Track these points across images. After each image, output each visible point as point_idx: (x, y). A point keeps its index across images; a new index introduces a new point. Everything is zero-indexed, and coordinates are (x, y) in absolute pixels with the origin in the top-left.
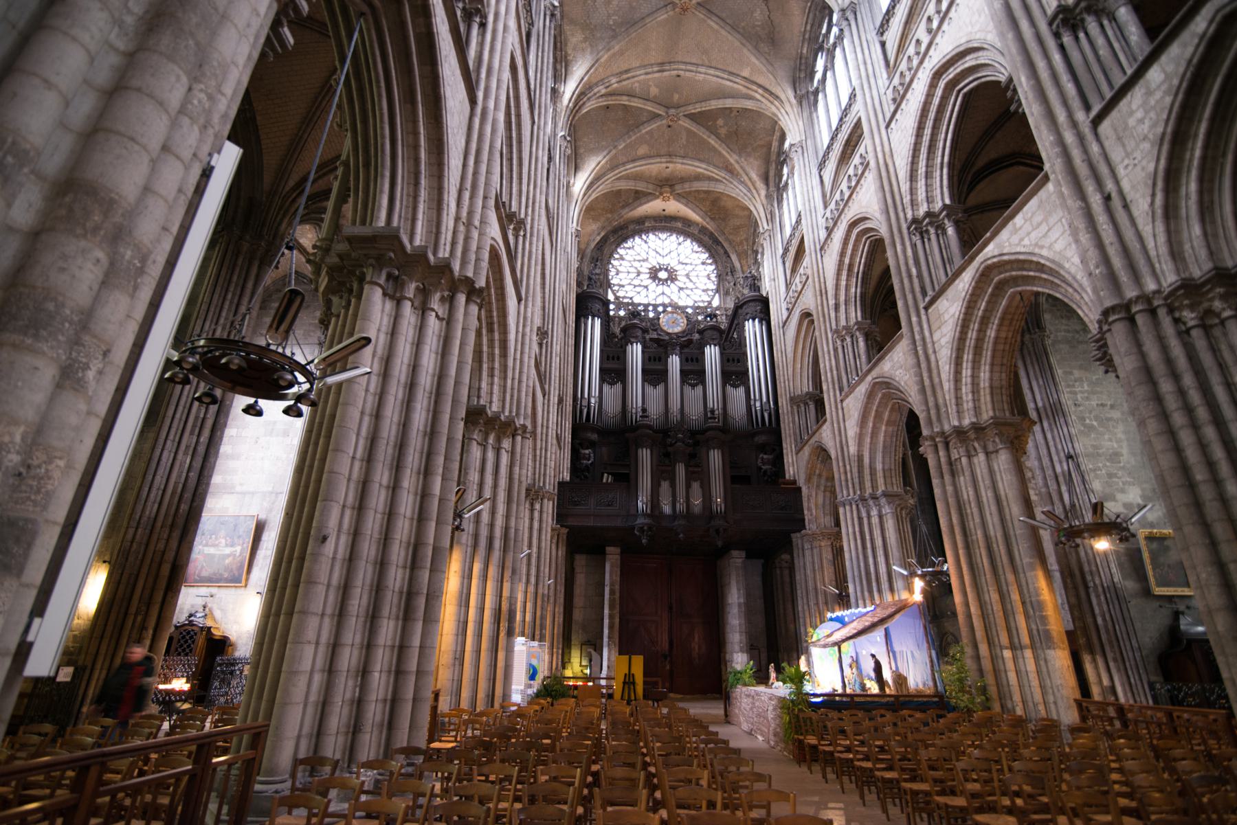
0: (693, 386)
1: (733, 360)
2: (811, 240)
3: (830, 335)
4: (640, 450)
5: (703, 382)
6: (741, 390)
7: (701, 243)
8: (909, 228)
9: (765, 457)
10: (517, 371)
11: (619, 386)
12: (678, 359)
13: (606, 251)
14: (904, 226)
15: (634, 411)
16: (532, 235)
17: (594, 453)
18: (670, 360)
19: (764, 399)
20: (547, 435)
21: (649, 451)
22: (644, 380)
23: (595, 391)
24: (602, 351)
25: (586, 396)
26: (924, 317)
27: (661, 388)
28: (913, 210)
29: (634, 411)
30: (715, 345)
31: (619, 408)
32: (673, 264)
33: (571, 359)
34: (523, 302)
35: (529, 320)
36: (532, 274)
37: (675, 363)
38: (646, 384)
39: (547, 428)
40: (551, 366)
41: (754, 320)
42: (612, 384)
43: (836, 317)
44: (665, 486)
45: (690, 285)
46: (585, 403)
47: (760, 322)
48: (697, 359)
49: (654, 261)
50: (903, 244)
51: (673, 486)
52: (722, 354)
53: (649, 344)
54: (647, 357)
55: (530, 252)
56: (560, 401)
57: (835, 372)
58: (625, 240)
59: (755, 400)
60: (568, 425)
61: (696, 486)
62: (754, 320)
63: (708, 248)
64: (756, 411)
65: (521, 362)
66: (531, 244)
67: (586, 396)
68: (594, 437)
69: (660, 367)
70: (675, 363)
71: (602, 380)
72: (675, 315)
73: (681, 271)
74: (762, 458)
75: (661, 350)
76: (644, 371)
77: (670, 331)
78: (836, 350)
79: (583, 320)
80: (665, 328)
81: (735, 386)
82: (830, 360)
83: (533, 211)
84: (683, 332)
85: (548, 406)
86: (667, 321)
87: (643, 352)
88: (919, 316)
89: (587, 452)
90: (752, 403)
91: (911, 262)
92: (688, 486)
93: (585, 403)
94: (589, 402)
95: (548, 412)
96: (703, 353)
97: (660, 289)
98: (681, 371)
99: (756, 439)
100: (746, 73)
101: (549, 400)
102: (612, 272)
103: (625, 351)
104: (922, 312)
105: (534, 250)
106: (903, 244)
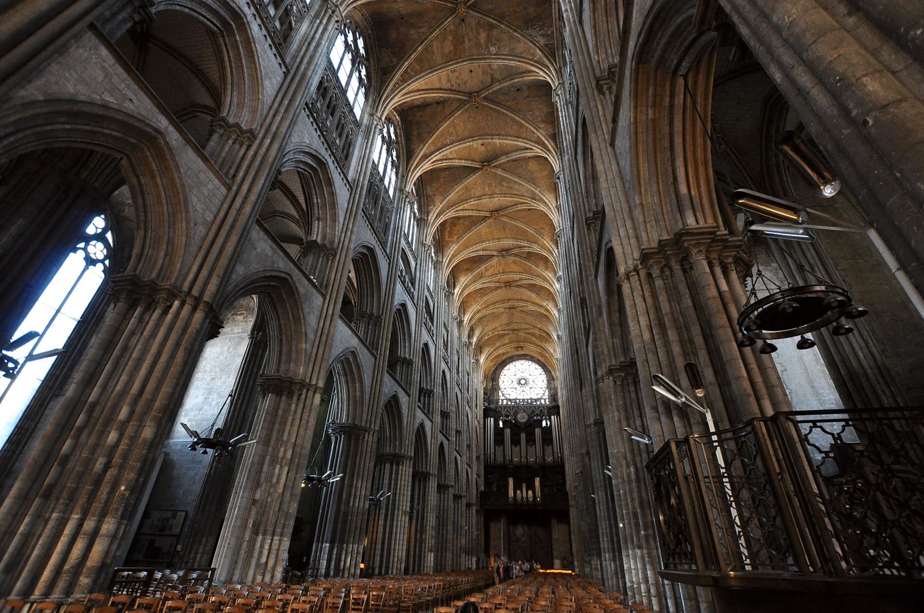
0: (531, 446)
7: (539, 364)
13: (497, 373)
23: (492, 451)
32: (527, 376)
37: (523, 436)
44: (519, 492)
45: (535, 386)
49: (519, 376)
51: (522, 492)
58: (505, 366)
60: (482, 467)
61: (530, 492)
63: (542, 368)
70: (523, 436)
71: (495, 444)
73: (531, 381)
92: (527, 493)
97: (522, 389)
100: (539, 326)
102: (501, 383)
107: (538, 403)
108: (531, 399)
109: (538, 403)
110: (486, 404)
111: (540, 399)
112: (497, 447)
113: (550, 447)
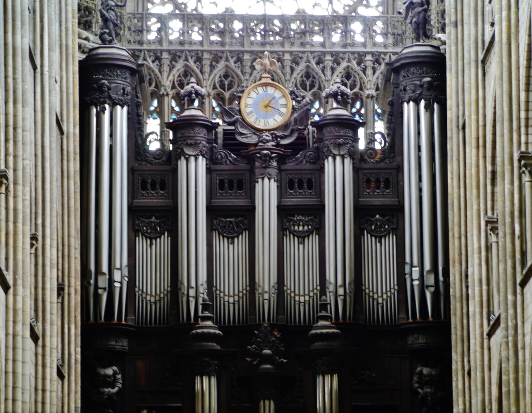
0: (302, 237)
1: (378, 181)
2: (473, 38)
3: (483, 223)
4: (198, 380)
5: (320, 230)
6: (390, 241)
8: (520, 161)
9: (425, 371)
10: (10, 389)
11: (165, 241)
12: (274, 185)
14: (516, 156)
15: (192, 293)
16: (15, 183)
17: (123, 373)
18: (258, 187)
19: (427, 266)
20: (43, 403)
21: (214, 380)
22: (210, 228)
24: (131, 171)
25: (105, 268)
26: (519, 297)
27: (242, 242)
28: (527, 134)
29: (192, 293)
30: (343, 157)
31: (166, 284)
33: (75, 203)
34: (11, 291)
35: (20, 313)
36: (20, 244)
38: (215, 235)
39: (44, 391)
40: (43, 289)
41: (417, 103)
42: (152, 237)
43: (493, 193)
46: (103, 282)
47: (429, 108)
48: (310, 181)
50: (512, 183)
52: (356, 170)
53: (222, 153)
54: (217, 179)
55: (15, 210)
56: (60, 289)
57: (485, 287)
59: (412, 266)
62: (417, 103)
64: (412, 286)
65: (14, 373)
66: (15, 197)
67: (105, 268)
68: (123, 344)
69: (241, 202)
72: (270, 90)
74: (421, 372)
75: (243, 165)
76: (211, 210)
77: (260, 125)
78: (488, 248)
79: (94, 111)
80: (251, 120)
81: (379, 237)
82: (480, 265)
83: (15, 142)
84: (285, 126)
85: (44, 356)
86: (255, 105)
87: (209, 171)
88: (515, 293)
89: (109, 371)
90: (407, 269)
91: (516, 213)
93: (103, 282)
94: (111, 281)
95: (44, 366)
96: (322, 169)
98: (281, 209)
99: (411, 340)
101: (44, 347)
103: (175, 171)
104: (518, 288)
105: (20, 207)
106: (512, 183)
107: (336, 38)
108: (301, 16)
109: (336, 38)
110: (94, 41)
111: (345, 20)
112: (141, 244)
113: (390, 241)
